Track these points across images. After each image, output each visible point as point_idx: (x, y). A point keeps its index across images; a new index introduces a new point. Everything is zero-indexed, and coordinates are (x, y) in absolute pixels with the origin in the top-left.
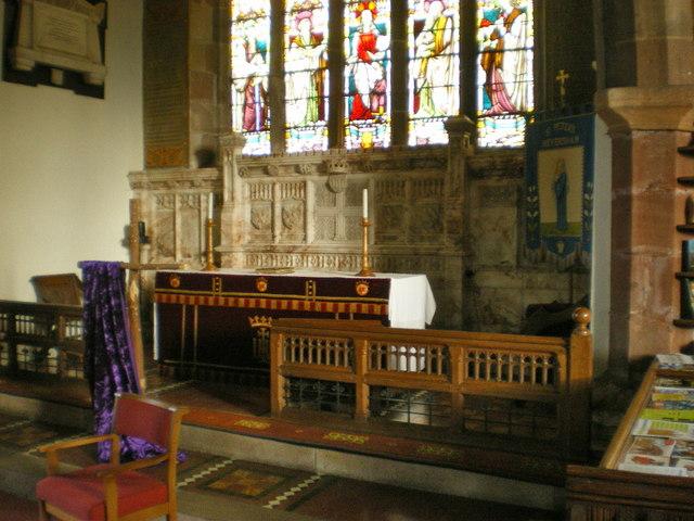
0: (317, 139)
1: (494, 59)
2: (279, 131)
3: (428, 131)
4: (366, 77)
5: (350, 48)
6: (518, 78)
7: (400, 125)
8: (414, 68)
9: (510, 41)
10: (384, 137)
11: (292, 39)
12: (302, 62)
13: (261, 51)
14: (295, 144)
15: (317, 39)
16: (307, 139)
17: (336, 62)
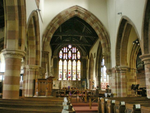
1: (78, 75)
2: (63, 78)
3: (74, 79)
4: (69, 75)
5: (68, 73)
6: (79, 76)
7: (72, 79)
8: (73, 75)
9: (79, 74)
10: (71, 79)
12: (65, 74)
13: (62, 72)
14: (64, 79)
15: (66, 72)
16: (65, 79)
17: (67, 74)
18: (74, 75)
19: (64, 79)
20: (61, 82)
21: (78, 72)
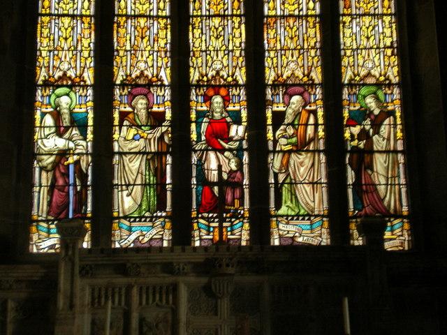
0: (156, 233)
1: (363, 158)
2: (104, 218)
7: (261, 222)
8: (276, 162)
9: (379, 143)
10: (241, 233)
11: (123, 115)
13: (83, 128)
15: (156, 119)
17: (180, 146)
18: (302, 165)
19: (125, 237)
20: (50, 283)
21: (356, 119)
